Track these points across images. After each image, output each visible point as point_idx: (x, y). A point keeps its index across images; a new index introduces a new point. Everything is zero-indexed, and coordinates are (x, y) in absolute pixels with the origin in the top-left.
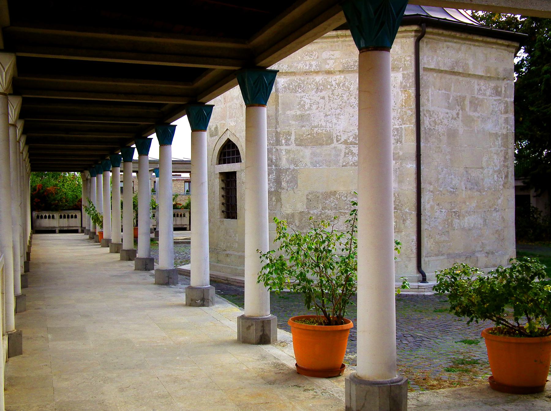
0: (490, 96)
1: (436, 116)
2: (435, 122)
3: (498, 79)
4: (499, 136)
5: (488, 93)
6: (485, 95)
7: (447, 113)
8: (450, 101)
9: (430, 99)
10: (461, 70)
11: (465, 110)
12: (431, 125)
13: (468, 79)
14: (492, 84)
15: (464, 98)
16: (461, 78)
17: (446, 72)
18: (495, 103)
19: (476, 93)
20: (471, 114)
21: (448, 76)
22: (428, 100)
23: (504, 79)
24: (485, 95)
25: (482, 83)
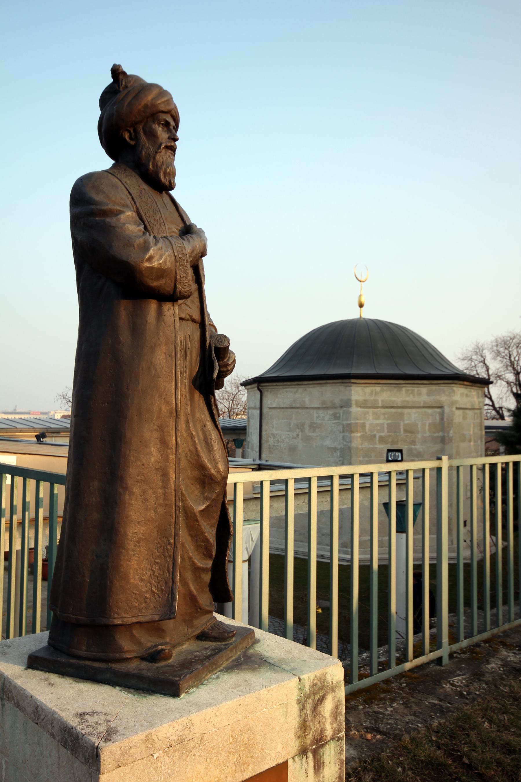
0: (328, 420)
1: (279, 437)
2: (278, 441)
3: (335, 408)
4: (338, 450)
5: (326, 418)
6: (324, 420)
7: (289, 435)
8: (291, 427)
9: (275, 426)
10: (298, 405)
11: (304, 432)
12: (274, 443)
13: (308, 410)
14: (331, 412)
15: (303, 424)
16: (300, 411)
17: (287, 408)
18: (333, 425)
19: (315, 419)
20: (310, 434)
21: (290, 410)
22: (273, 427)
23: (341, 407)
24: (324, 420)
25: (321, 412)
